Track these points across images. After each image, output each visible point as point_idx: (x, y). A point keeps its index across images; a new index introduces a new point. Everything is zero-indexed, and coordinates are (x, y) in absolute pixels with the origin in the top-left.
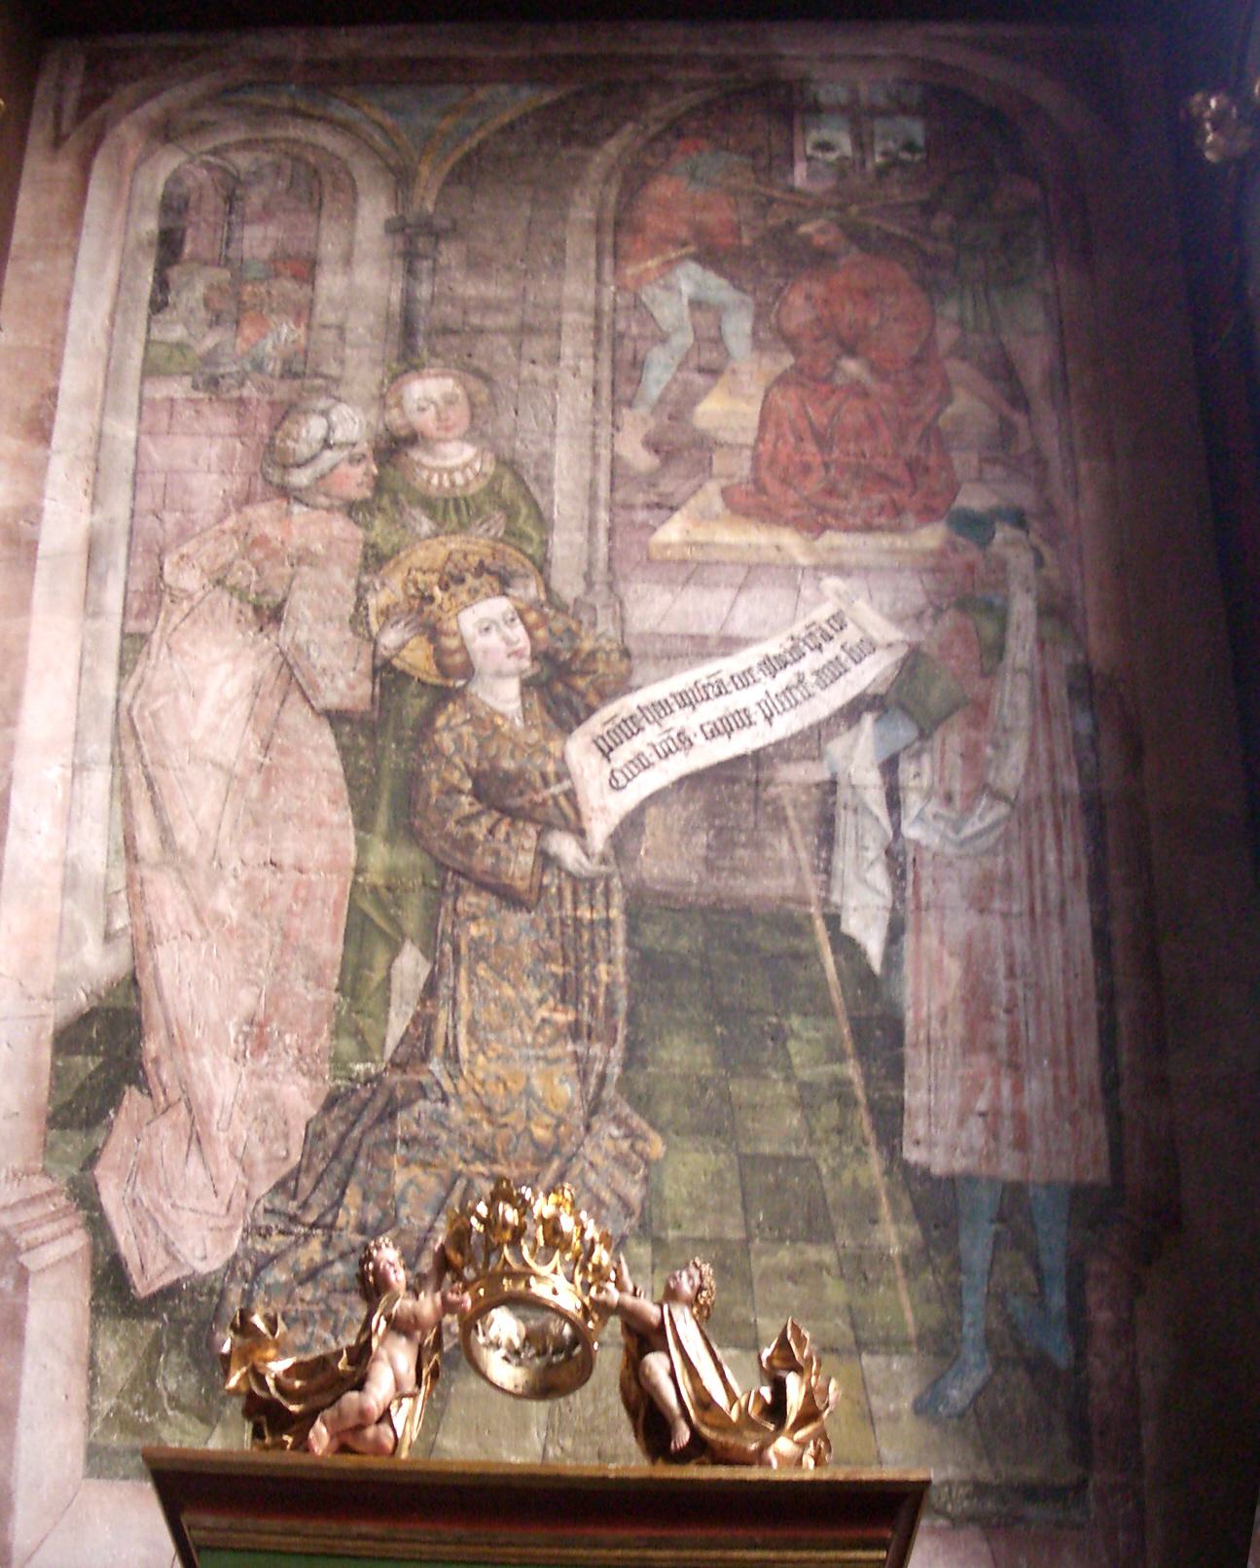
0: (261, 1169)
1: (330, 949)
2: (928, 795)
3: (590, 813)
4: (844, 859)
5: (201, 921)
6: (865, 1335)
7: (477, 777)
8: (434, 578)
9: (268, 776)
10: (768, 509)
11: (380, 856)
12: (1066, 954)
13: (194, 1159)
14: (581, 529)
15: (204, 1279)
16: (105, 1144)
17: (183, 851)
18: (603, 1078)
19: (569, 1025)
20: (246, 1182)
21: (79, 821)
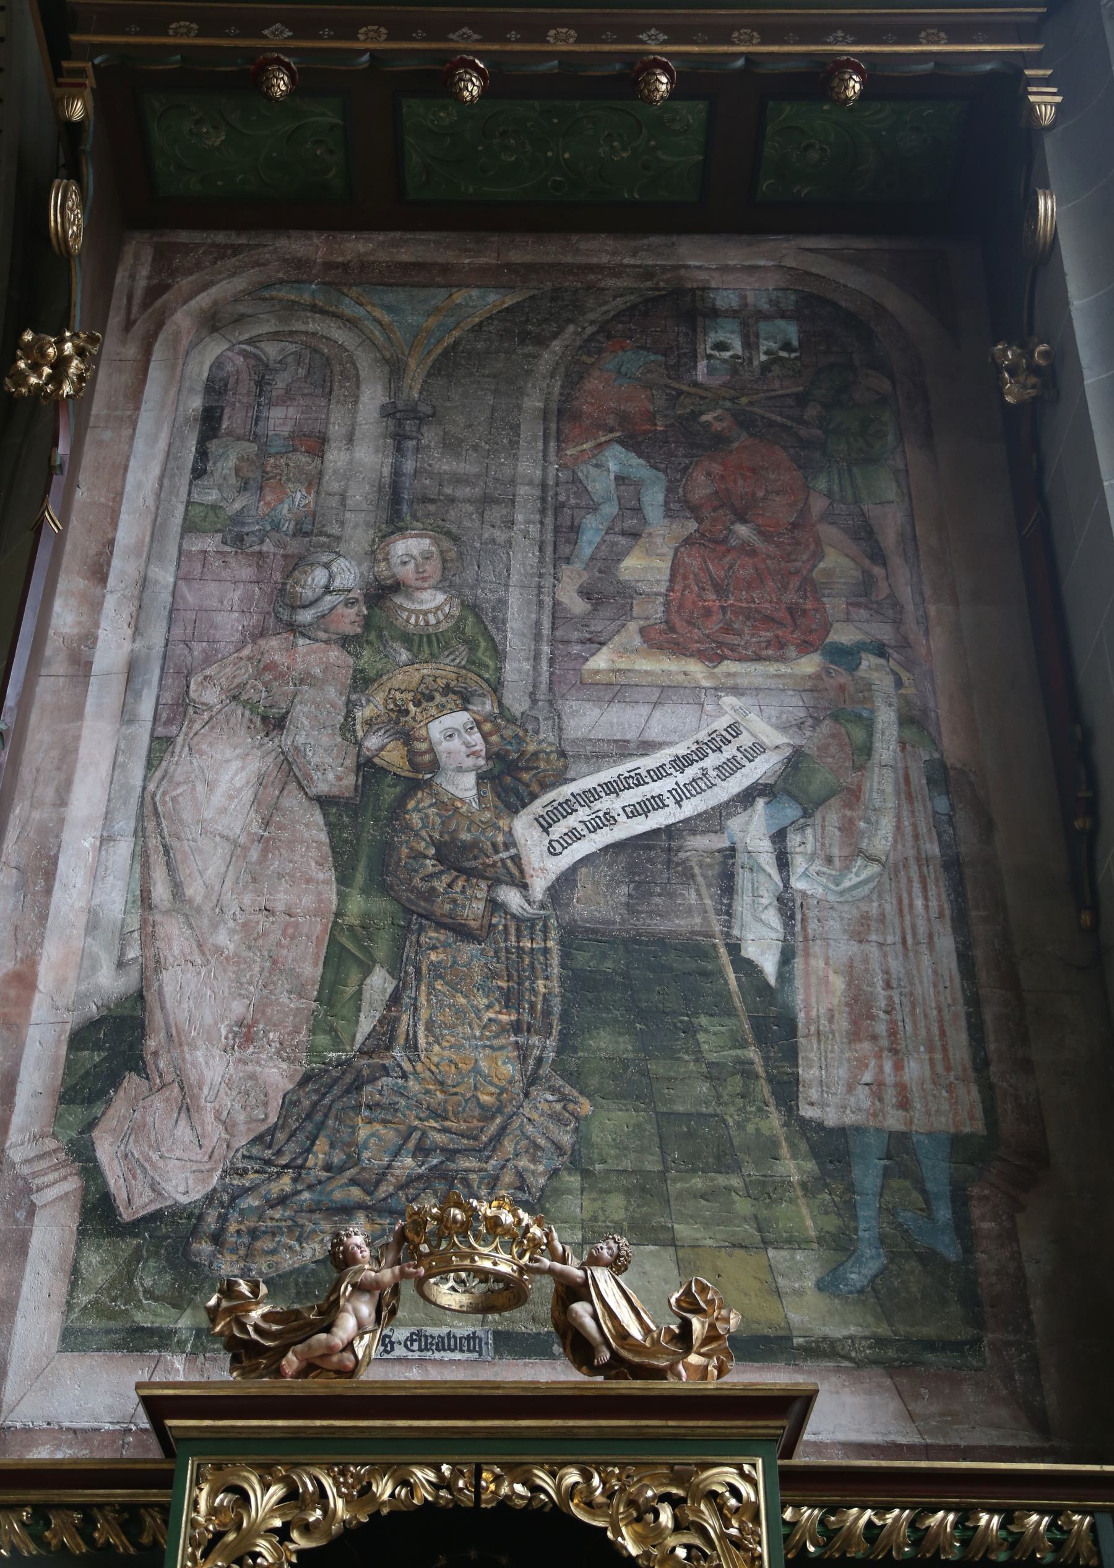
0: (242, 1128)
1: (311, 971)
2: (812, 858)
3: (532, 872)
4: (743, 904)
5: (203, 954)
6: (770, 1236)
7: (439, 846)
8: (410, 696)
9: (267, 845)
10: (678, 644)
11: (357, 904)
12: (935, 972)
13: (183, 1123)
14: (528, 659)
15: (185, 1207)
16: (103, 1114)
17: (190, 901)
18: (540, 1060)
19: (512, 1023)
20: (227, 1137)
21: (103, 878)
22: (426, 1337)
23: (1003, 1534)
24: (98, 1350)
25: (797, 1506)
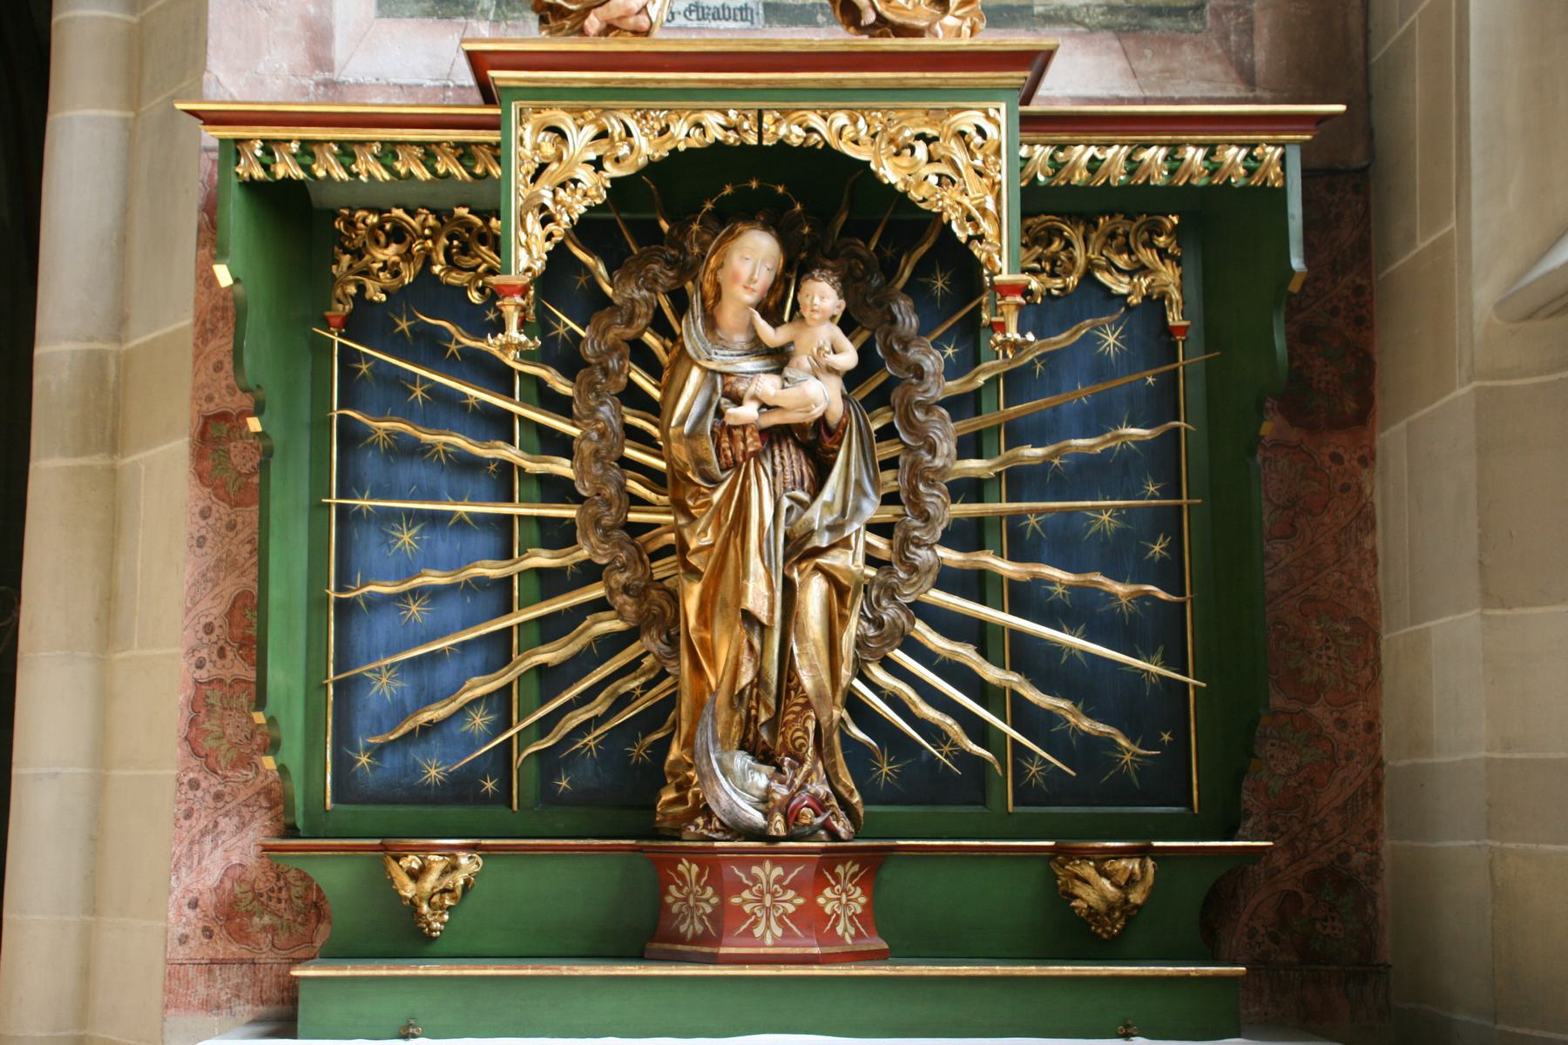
22: (703, 9)
23: (1206, 163)
24: (412, 17)
25: (1032, 144)
